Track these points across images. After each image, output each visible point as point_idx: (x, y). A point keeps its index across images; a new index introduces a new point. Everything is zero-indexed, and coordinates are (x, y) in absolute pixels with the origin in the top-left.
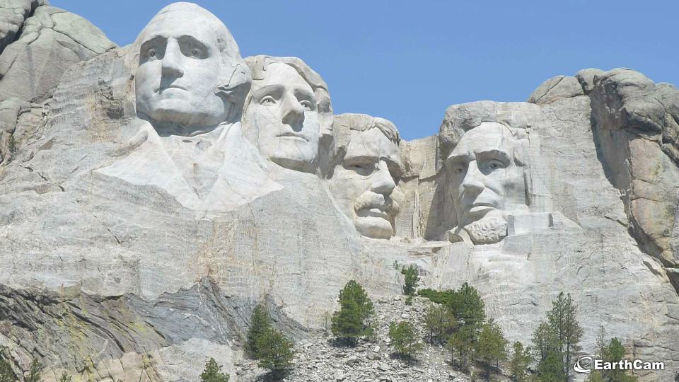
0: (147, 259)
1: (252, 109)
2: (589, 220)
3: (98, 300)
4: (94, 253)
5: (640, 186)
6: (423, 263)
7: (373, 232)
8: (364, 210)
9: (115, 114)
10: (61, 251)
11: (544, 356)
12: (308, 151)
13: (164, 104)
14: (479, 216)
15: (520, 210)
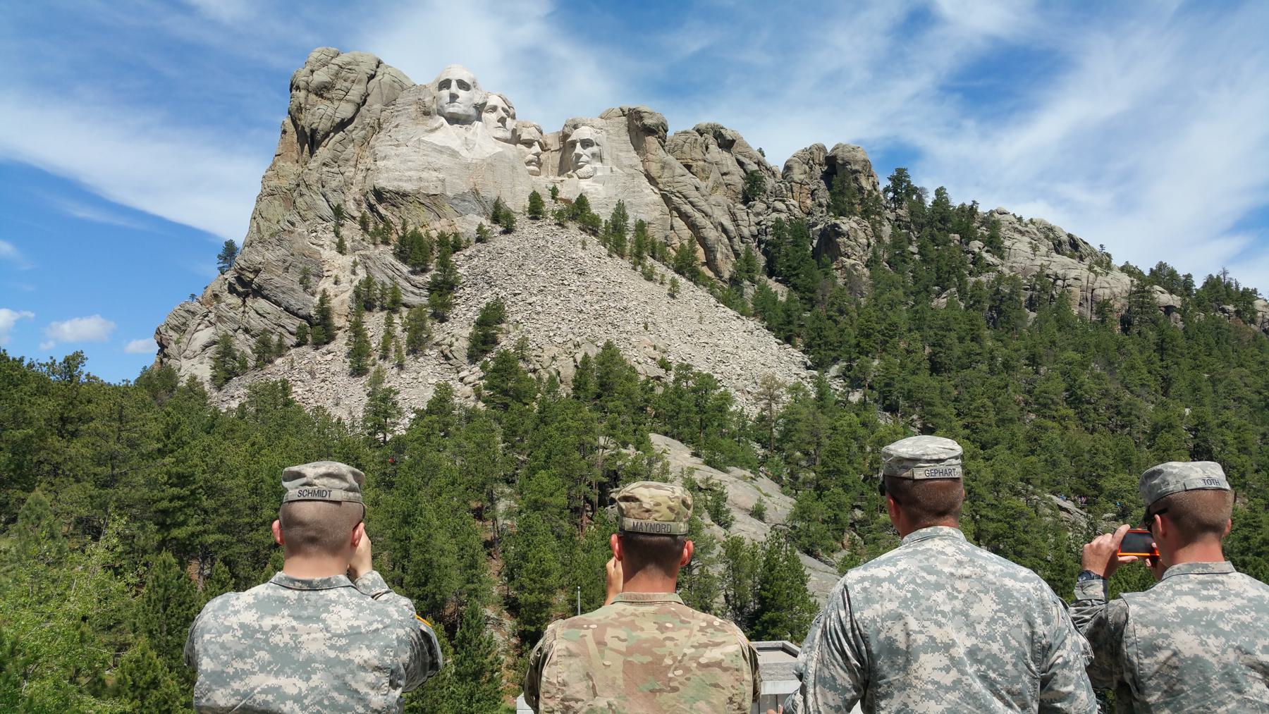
0: (448, 179)
1: (484, 115)
2: (628, 170)
3: (428, 196)
4: (425, 175)
5: (650, 156)
6: (559, 186)
7: (532, 173)
8: (529, 163)
9: (427, 113)
10: (409, 173)
11: (615, 227)
12: (508, 135)
13: (451, 109)
14: (581, 167)
15: (598, 165)
